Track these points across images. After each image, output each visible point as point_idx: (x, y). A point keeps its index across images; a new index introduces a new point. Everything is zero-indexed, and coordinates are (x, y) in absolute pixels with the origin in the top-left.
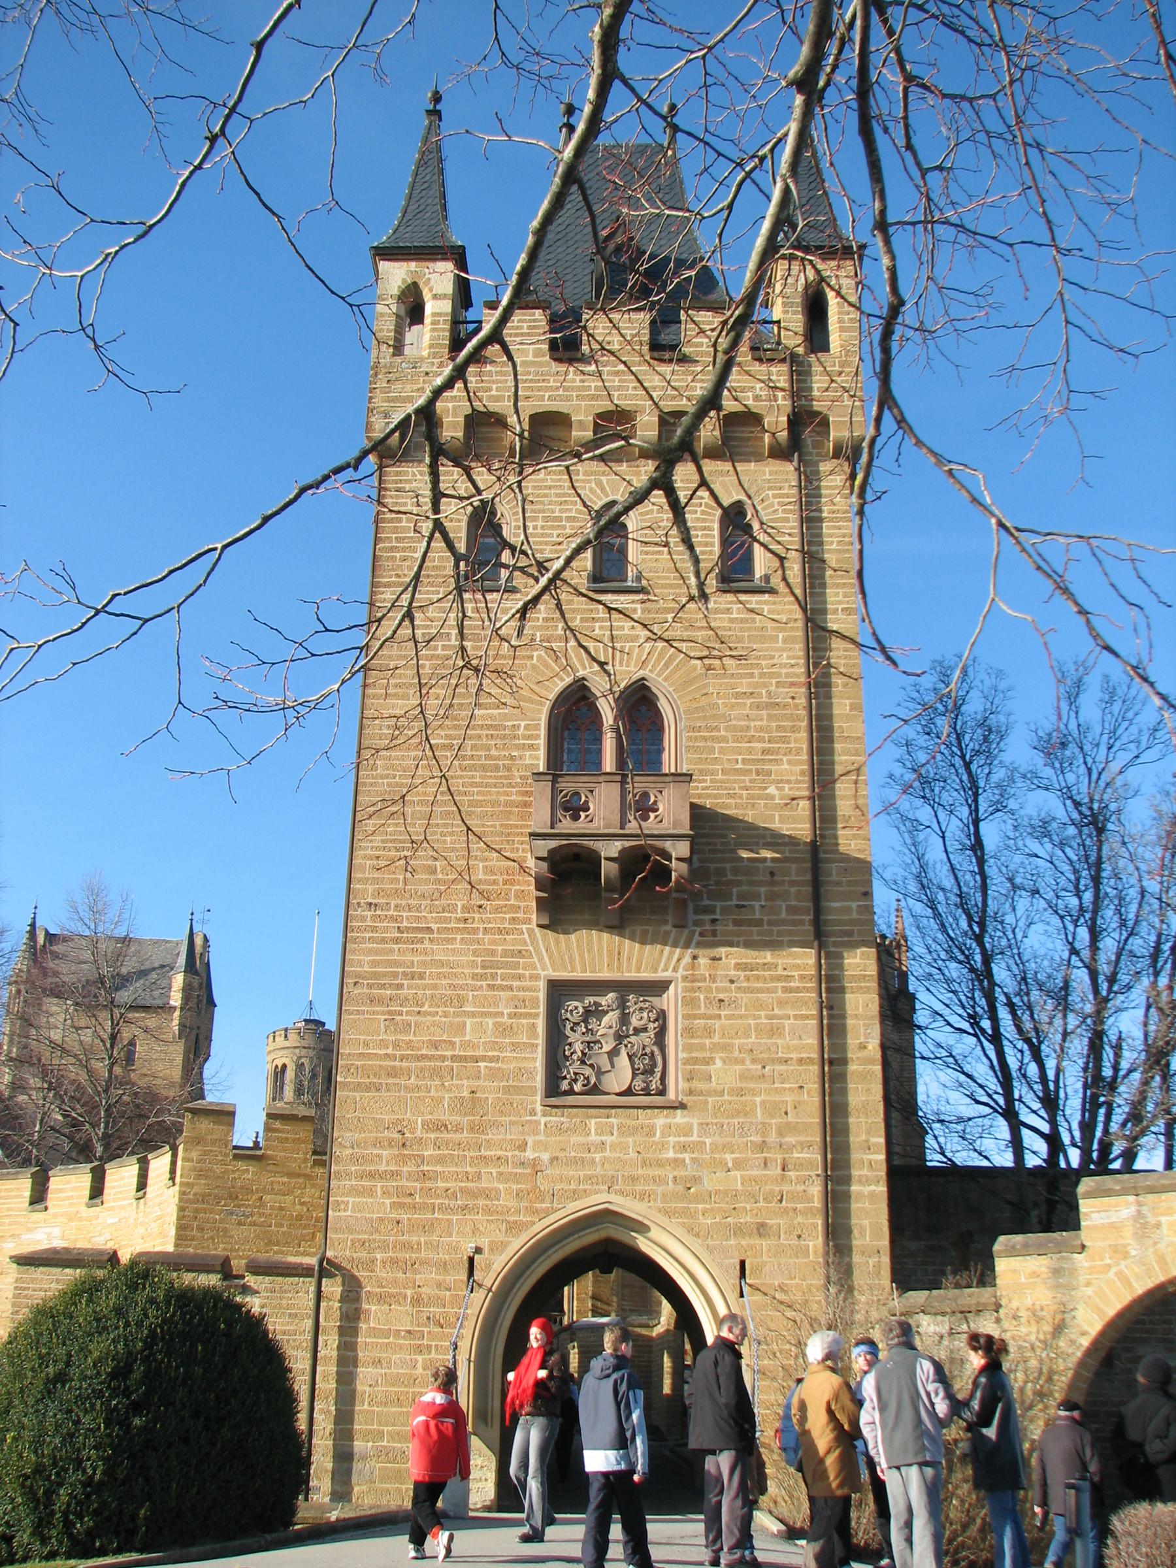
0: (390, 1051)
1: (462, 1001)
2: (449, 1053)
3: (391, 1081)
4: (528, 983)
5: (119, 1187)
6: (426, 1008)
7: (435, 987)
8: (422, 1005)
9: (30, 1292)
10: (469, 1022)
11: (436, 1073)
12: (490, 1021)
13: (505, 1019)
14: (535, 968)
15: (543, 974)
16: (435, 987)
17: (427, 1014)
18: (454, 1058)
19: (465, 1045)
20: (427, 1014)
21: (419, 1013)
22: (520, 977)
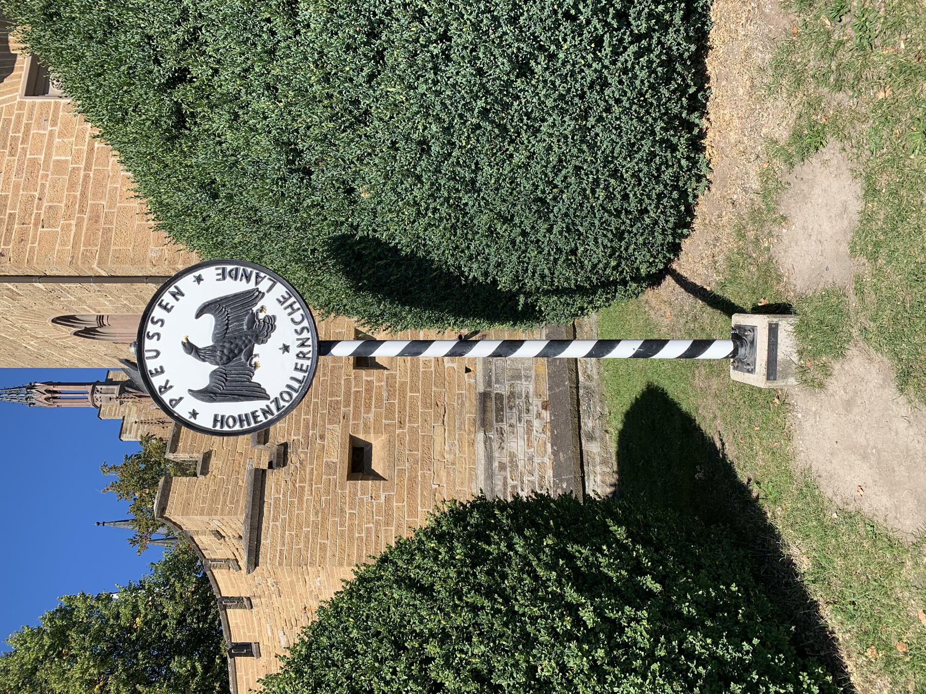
0: (73, 222)
1: (34, 162)
2: (82, 173)
3: (102, 220)
4: (26, 112)
5: (243, 627)
6: (37, 194)
7: (17, 186)
8: (33, 197)
9: (285, 548)
10: (55, 158)
11: (99, 184)
12: (57, 140)
13: (57, 129)
14: (12, 106)
15: (18, 99)
16: (17, 186)
17: (42, 192)
18: (88, 167)
19: (77, 158)
20: (42, 192)
21: (40, 199)
22: (19, 117)
